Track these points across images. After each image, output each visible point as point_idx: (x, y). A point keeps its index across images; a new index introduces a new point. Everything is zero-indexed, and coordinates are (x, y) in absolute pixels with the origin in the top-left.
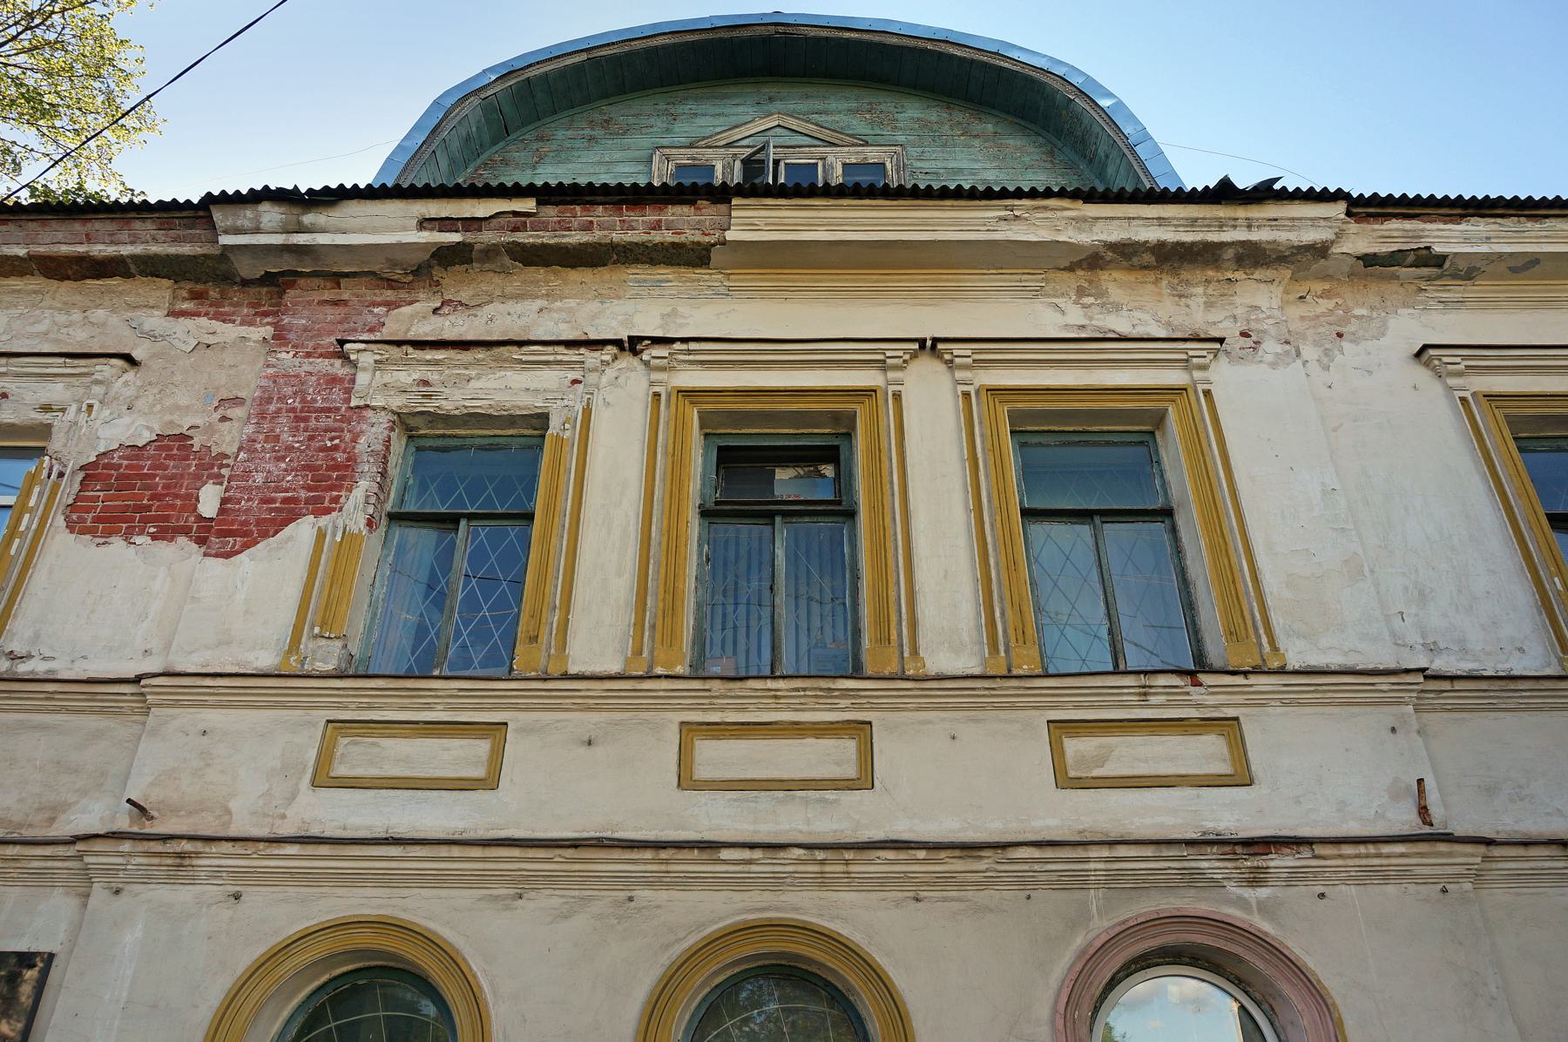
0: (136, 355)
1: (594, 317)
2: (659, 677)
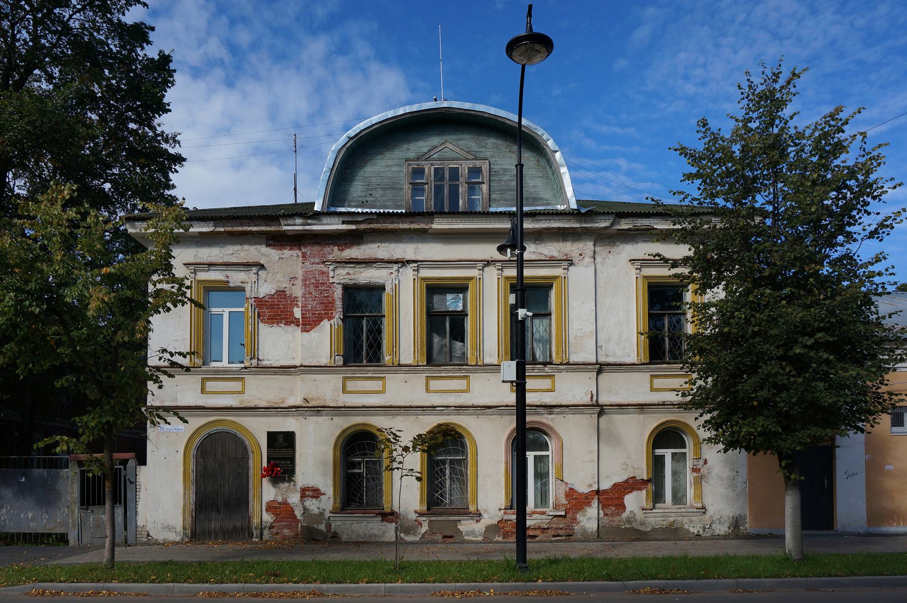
0: (262, 262)
1: (394, 249)
2: (420, 366)
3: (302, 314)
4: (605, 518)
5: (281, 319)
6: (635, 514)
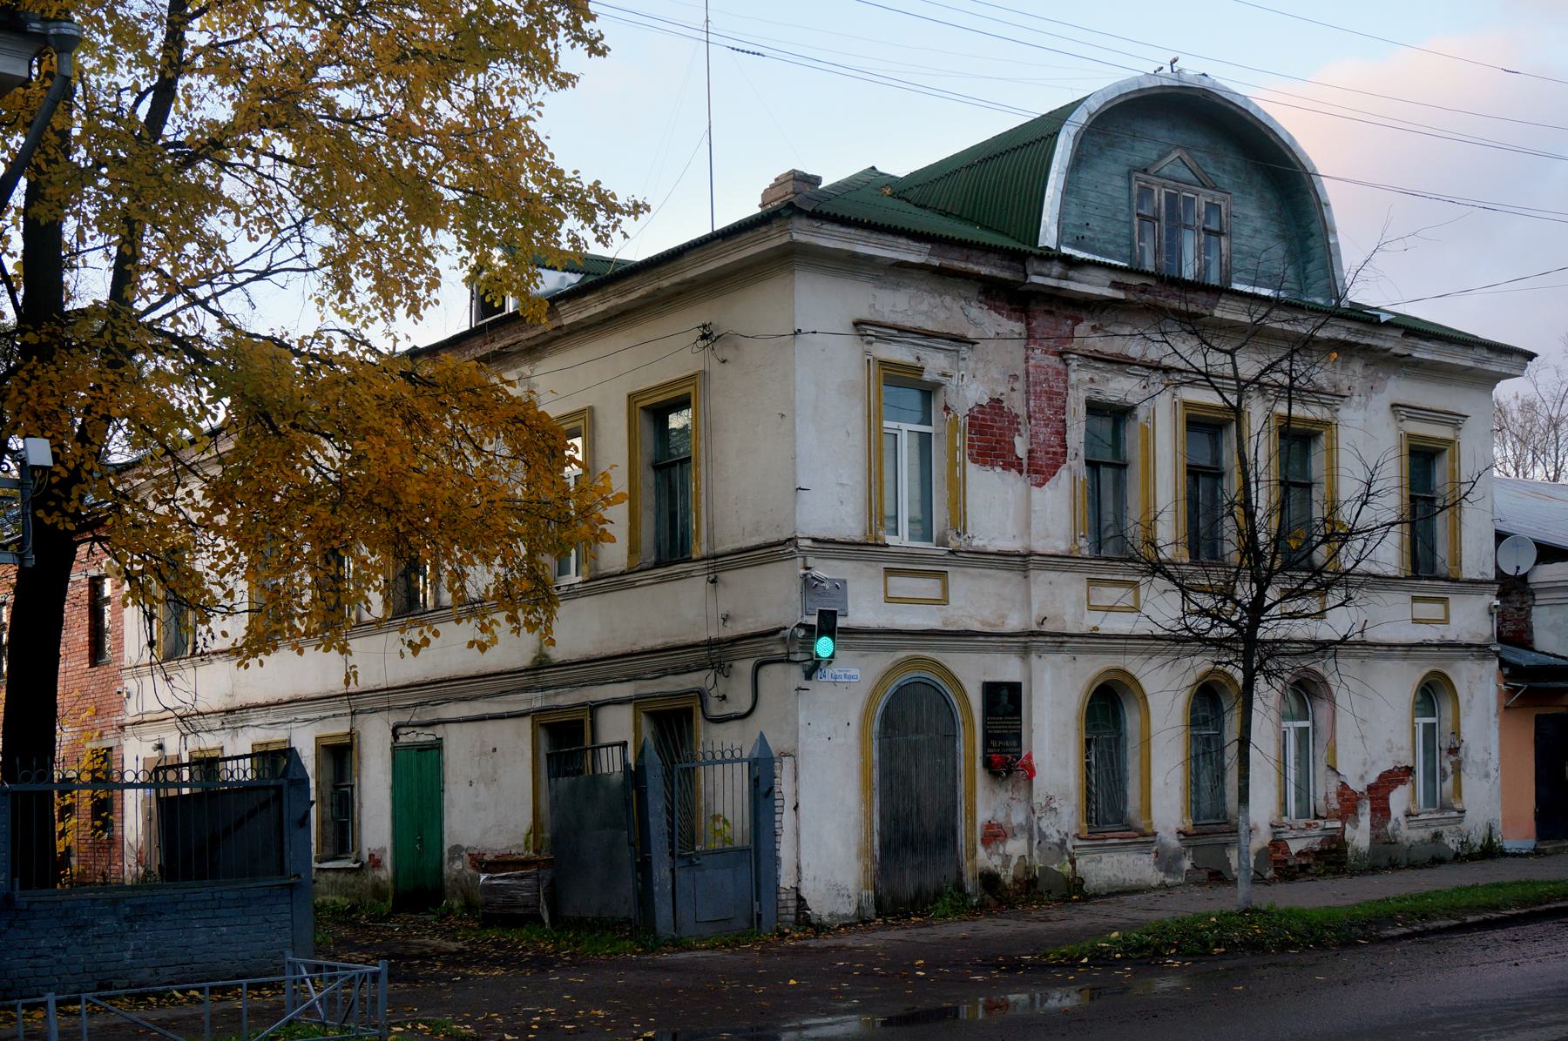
3: (1030, 452)
5: (997, 456)
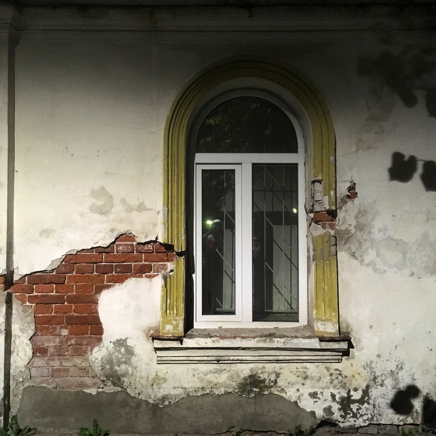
4: (39, 362)
6: (130, 352)
